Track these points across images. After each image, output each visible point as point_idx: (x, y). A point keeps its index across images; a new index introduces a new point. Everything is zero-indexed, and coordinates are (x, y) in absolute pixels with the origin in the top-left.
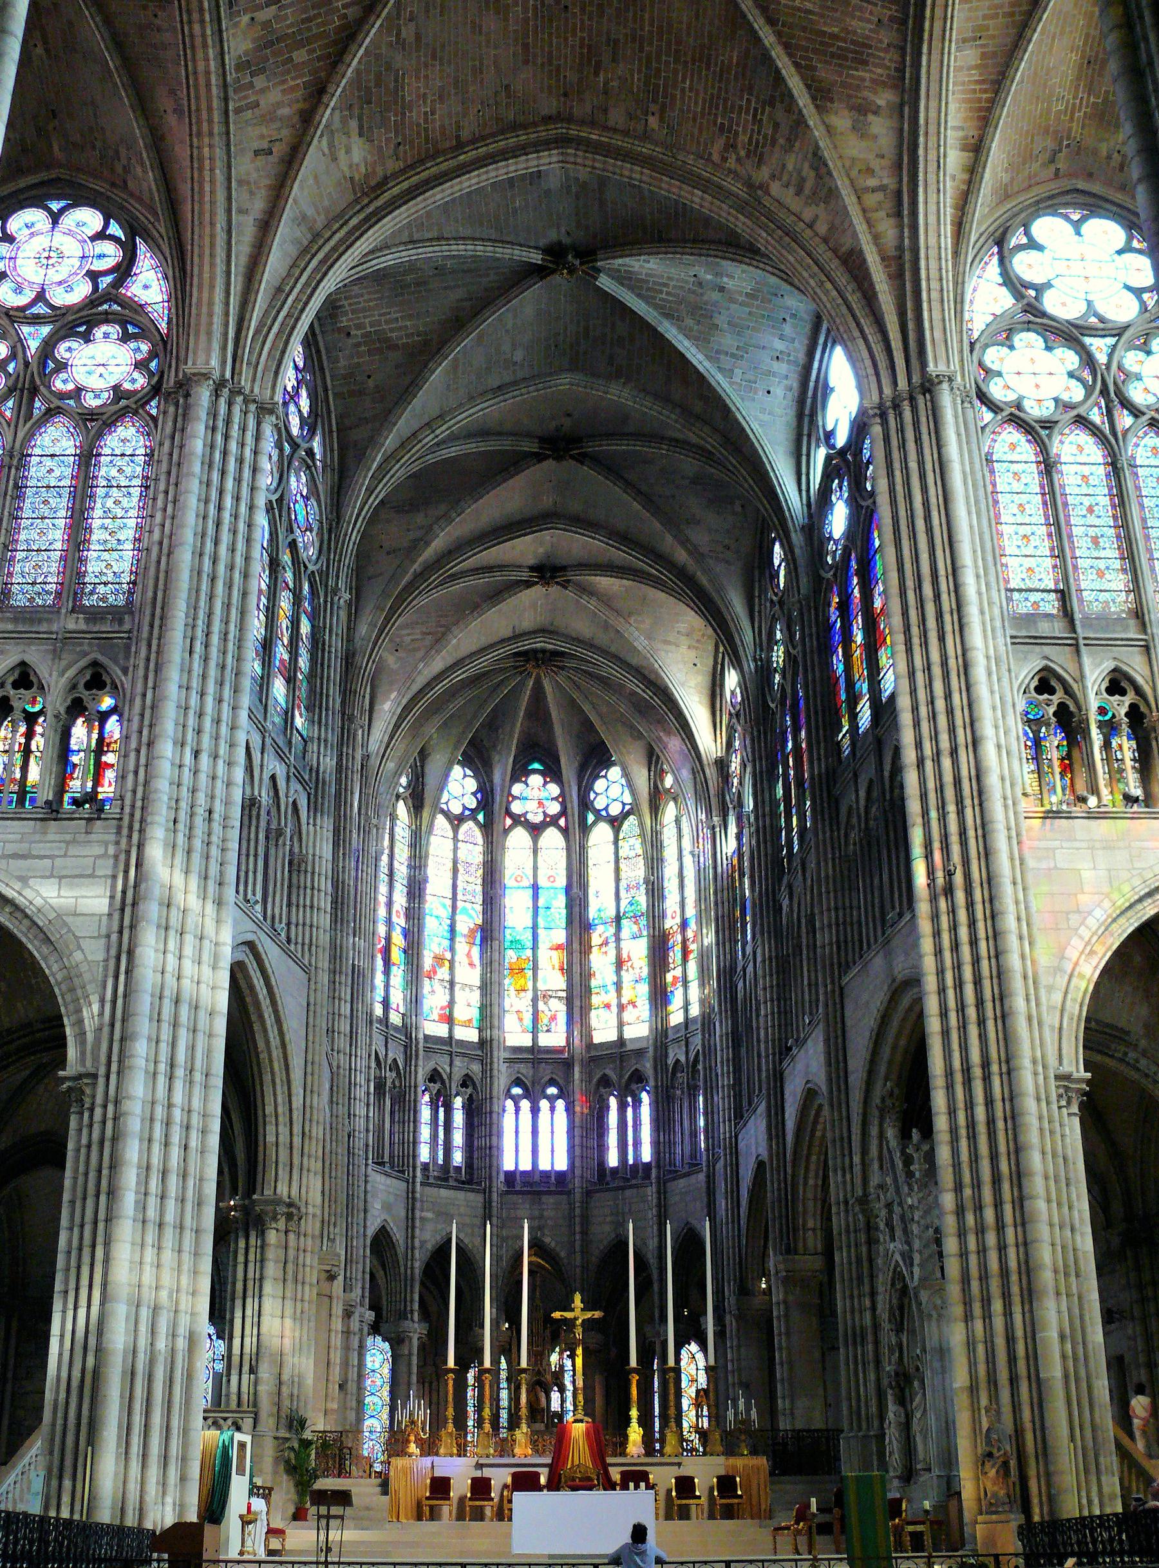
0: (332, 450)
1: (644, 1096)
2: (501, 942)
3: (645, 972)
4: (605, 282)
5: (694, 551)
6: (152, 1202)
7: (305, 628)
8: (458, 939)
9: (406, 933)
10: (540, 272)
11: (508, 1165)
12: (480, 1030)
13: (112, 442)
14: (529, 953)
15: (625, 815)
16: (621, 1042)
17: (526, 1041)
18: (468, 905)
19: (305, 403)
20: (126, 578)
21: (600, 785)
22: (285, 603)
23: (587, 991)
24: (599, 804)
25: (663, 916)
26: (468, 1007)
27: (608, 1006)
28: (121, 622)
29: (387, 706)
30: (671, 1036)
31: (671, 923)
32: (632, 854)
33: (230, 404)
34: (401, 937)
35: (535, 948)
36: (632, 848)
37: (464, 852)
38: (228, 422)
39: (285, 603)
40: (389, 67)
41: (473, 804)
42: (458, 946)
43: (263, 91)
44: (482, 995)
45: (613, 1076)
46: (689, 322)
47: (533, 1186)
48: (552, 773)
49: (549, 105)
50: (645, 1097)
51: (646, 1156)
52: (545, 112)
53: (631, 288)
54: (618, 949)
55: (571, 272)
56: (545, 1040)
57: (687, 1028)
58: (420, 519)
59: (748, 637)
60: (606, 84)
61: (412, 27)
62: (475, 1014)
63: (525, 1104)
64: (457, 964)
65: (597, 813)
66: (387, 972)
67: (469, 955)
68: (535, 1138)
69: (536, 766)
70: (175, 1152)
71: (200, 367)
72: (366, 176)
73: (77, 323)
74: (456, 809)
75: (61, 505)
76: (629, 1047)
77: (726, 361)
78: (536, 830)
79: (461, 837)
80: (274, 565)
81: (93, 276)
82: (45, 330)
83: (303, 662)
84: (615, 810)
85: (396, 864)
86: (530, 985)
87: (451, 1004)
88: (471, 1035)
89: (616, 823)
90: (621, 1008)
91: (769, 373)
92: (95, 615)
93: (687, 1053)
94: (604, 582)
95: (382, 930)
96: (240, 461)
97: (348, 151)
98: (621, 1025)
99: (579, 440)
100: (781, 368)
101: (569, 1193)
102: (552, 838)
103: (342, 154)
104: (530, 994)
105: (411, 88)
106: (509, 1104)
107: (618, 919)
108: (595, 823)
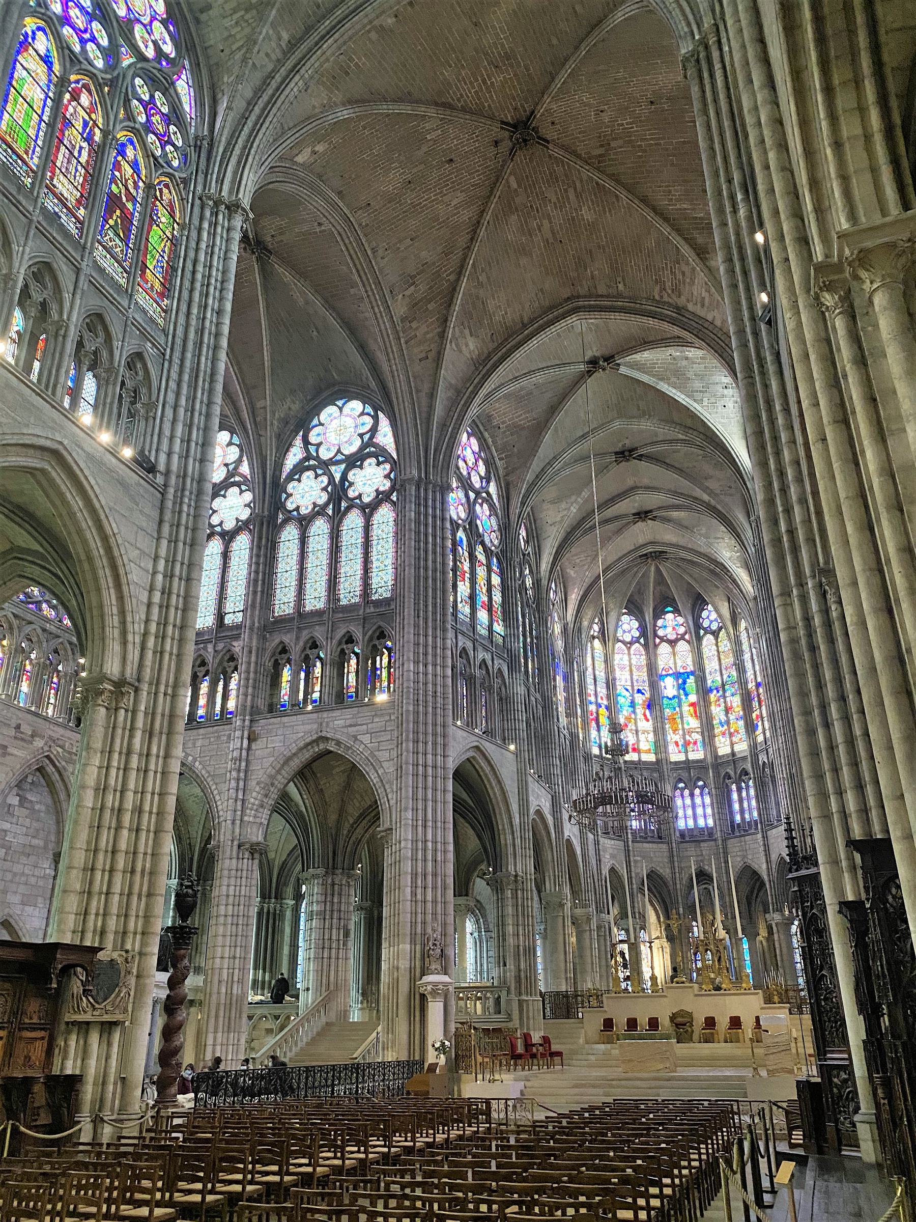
1: (751, 783)
3: (741, 713)
4: (623, 370)
5: (711, 493)
6: (419, 891)
7: (496, 580)
9: (607, 708)
10: (590, 373)
11: (681, 824)
13: (377, 518)
15: (720, 629)
16: (733, 754)
17: (682, 757)
19: (482, 469)
20: (390, 583)
21: (705, 614)
22: (481, 572)
24: (706, 624)
25: (746, 683)
26: (646, 742)
27: (724, 734)
28: (389, 605)
29: (573, 596)
31: (751, 685)
33: (426, 490)
36: (726, 646)
38: (426, 500)
39: (481, 572)
40: (478, 298)
41: (637, 634)
43: (417, 328)
45: (732, 773)
46: (673, 379)
47: (694, 837)
48: (677, 611)
49: (566, 293)
50: (751, 783)
51: (755, 814)
52: (566, 296)
53: (638, 369)
54: (725, 702)
55: (604, 370)
56: (693, 756)
58: (563, 505)
59: (749, 533)
62: (653, 748)
63: (686, 792)
65: (704, 629)
66: (599, 730)
67: (645, 715)
68: (694, 811)
69: (669, 609)
70: (430, 864)
71: (408, 476)
73: (354, 461)
74: (628, 638)
75: (359, 552)
77: (698, 396)
78: (673, 643)
79: (632, 652)
80: (472, 557)
81: (361, 436)
82: (343, 466)
83: (497, 598)
84: (714, 626)
85: (597, 673)
87: (638, 741)
88: (651, 758)
89: (715, 634)
90: (731, 735)
91: (723, 396)
92: (378, 603)
94: (675, 514)
95: (592, 708)
96: (434, 517)
97: (467, 345)
98: (732, 744)
99: (636, 449)
100: (729, 392)
101: (715, 840)
102: (682, 646)
104: (681, 732)
105: (491, 304)
106: (678, 792)
107: (723, 685)
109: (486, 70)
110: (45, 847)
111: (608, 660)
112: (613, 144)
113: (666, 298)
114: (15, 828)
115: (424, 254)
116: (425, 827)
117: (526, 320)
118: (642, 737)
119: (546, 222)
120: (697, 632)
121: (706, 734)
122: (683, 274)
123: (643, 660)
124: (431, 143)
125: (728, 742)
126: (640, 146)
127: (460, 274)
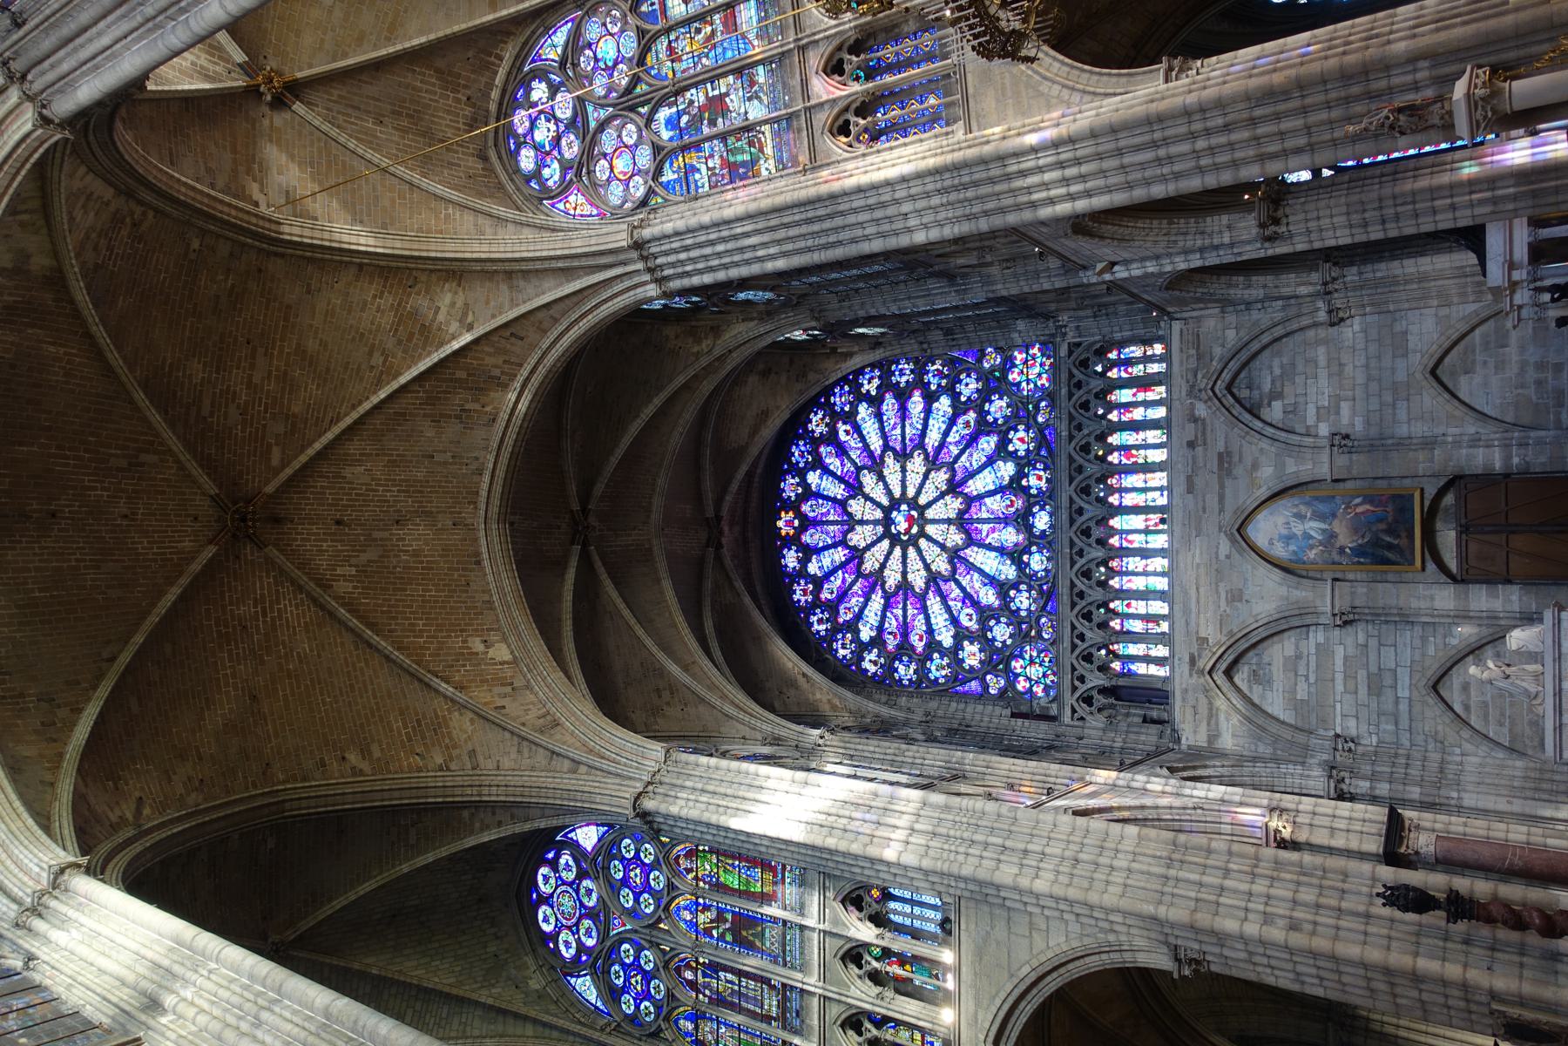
0: (533, 32)
4: (239, 56)
40: (400, 342)
43: (496, 366)
52: (279, 261)
60: (226, 280)
61: (373, 362)
72: (446, 280)
103: (459, 304)
105: (387, 320)
109: (257, 626)
110: (1326, 342)
112: (124, 463)
113: (138, 210)
114: (1312, 397)
115: (430, 433)
116: (1170, 159)
117: (353, 270)
119: (256, 379)
122: (95, 249)
124: (353, 561)
126: (86, 451)
127: (403, 389)
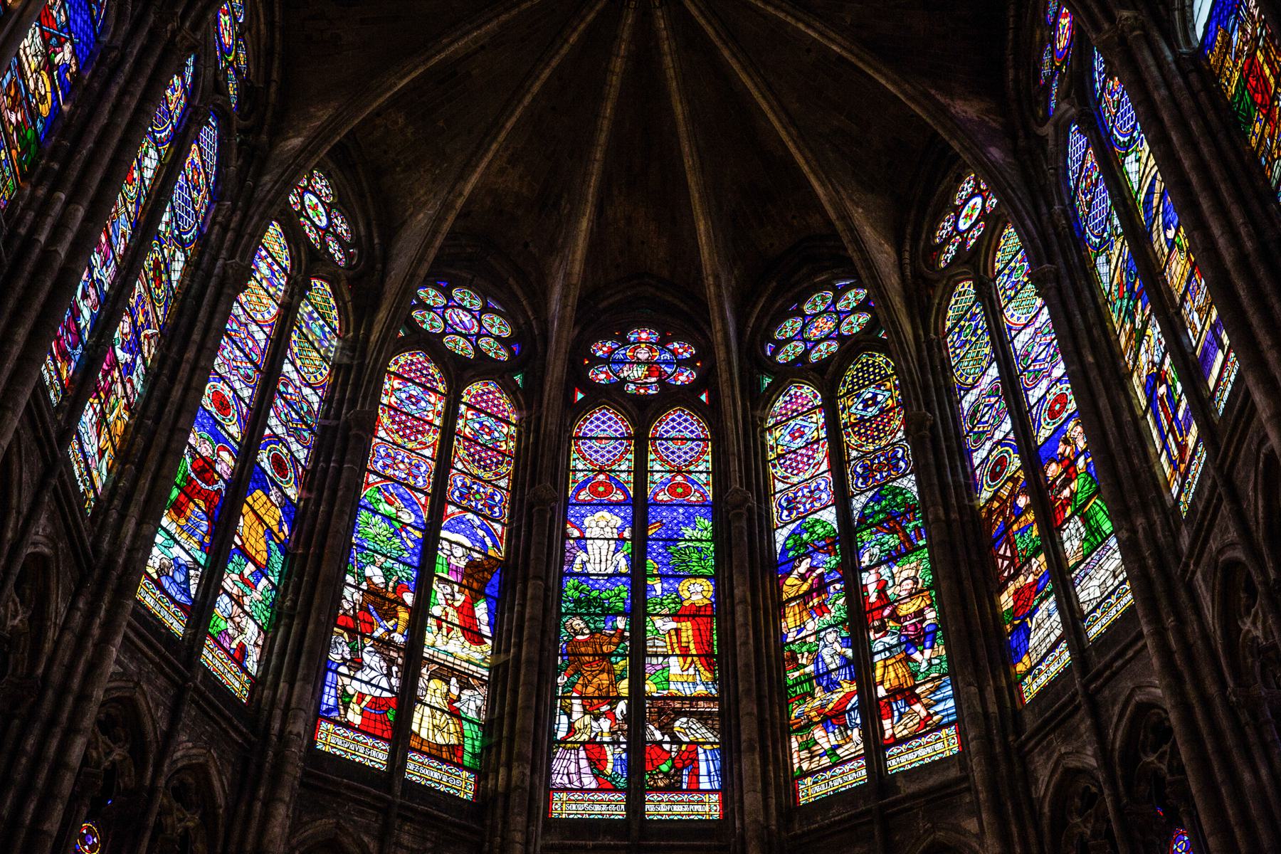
2: (552, 596)
8: (441, 571)
12: (480, 775)
14: (621, 623)
18: (470, 516)
23: (779, 695)
30: (1030, 723)
32: (873, 411)
34: (279, 512)
35: (638, 611)
37: (467, 424)
42: (439, 592)
44: (491, 700)
48: (679, 314)
54: (854, 591)
57: (1084, 672)
64: (431, 621)
67: (467, 612)
74: (459, 346)
76: (908, 788)
78: (641, 413)
86: (624, 687)
87: (407, 698)
89: (827, 377)
90: (872, 711)
93: (1099, 730)
98: (876, 747)
104: (622, 706)
108: (779, 387)
111: (354, 385)
118: (433, 690)
120: (734, 405)
121: (748, 706)
123: (505, 435)
125: (855, 742)
